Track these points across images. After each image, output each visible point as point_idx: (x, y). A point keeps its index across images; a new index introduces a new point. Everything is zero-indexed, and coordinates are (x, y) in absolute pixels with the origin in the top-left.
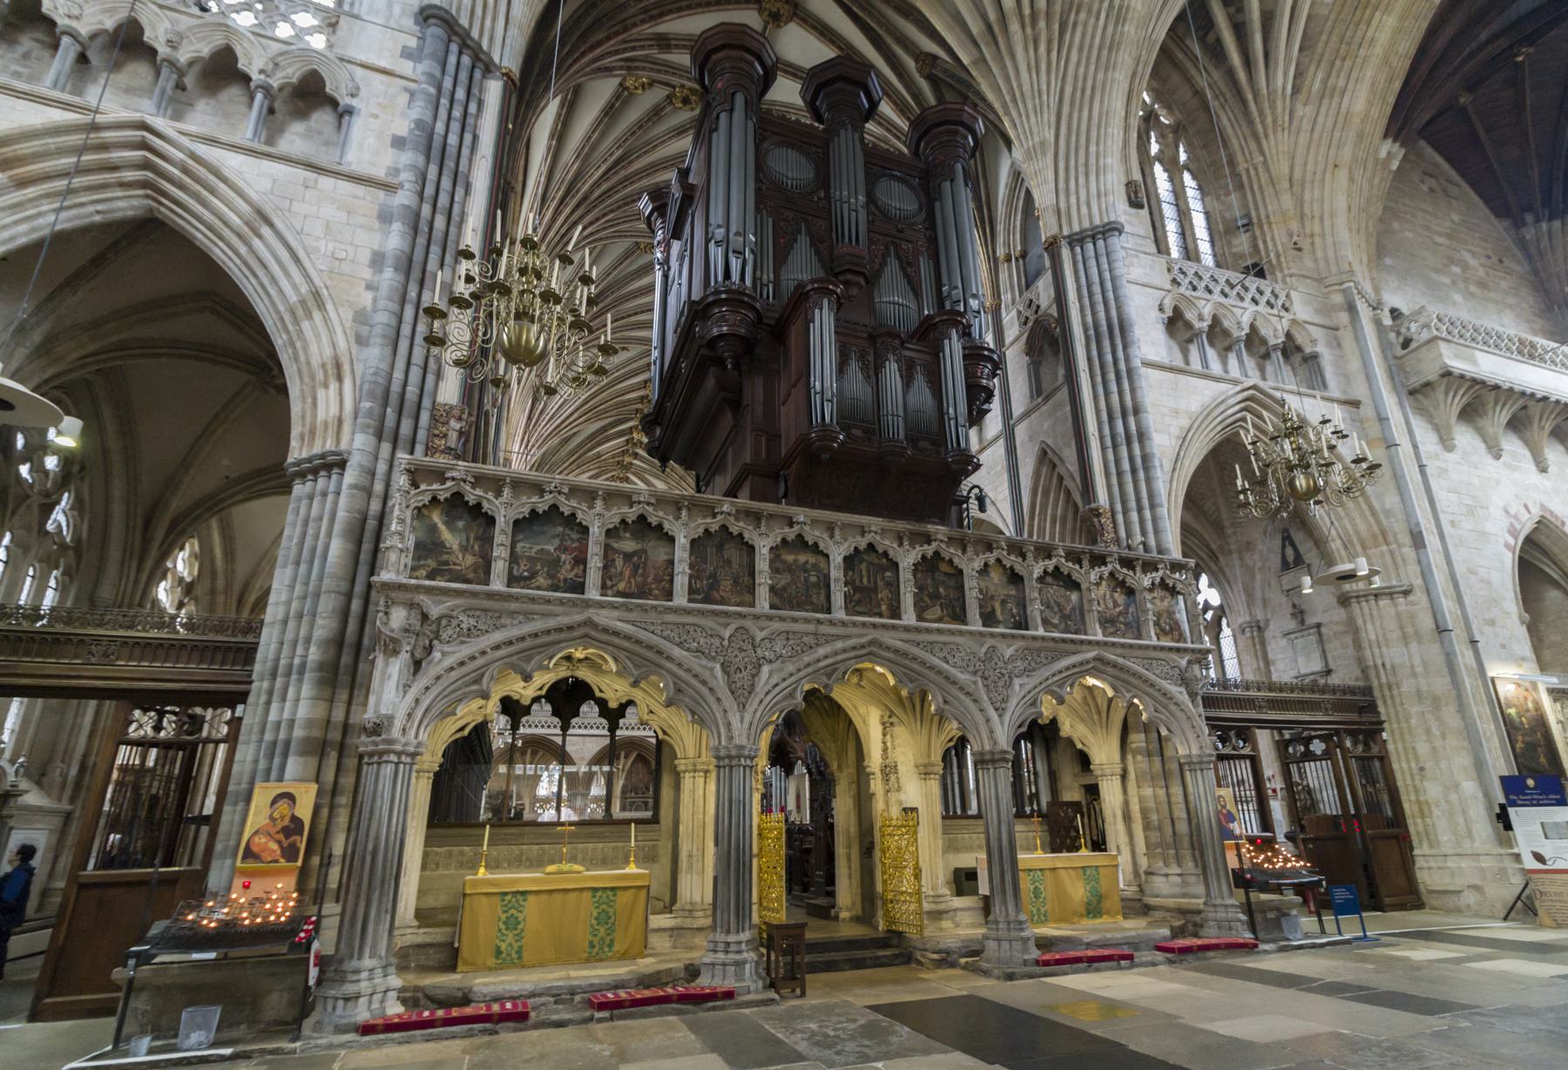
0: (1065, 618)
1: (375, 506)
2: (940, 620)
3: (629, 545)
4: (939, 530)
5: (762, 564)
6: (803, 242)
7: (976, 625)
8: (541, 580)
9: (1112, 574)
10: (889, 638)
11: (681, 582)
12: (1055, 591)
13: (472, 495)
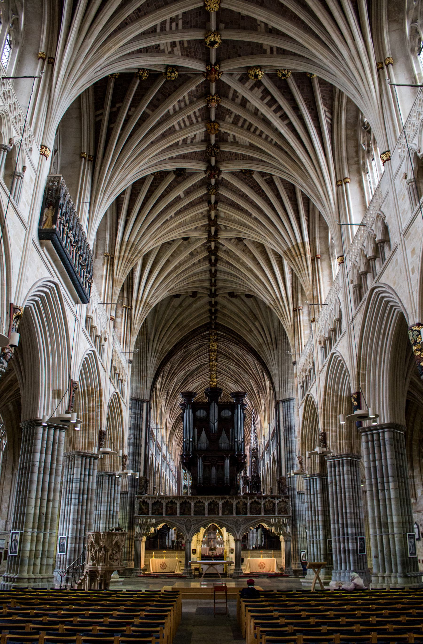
0: (257, 511)
1: (133, 499)
2: (227, 514)
3: (170, 505)
4: (228, 497)
5: (192, 507)
6: (203, 432)
7: (235, 515)
8: (157, 513)
9: (269, 500)
10: (216, 519)
11: (178, 511)
12: (254, 506)
13: (146, 500)
